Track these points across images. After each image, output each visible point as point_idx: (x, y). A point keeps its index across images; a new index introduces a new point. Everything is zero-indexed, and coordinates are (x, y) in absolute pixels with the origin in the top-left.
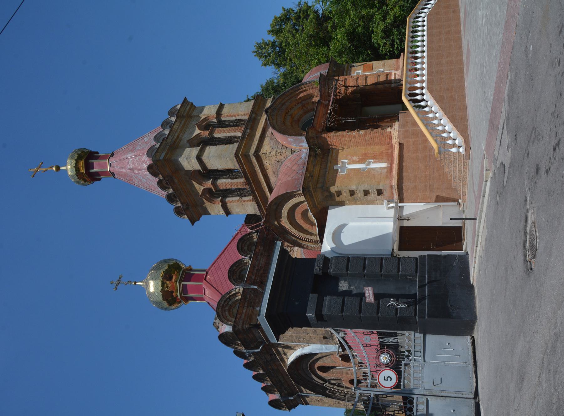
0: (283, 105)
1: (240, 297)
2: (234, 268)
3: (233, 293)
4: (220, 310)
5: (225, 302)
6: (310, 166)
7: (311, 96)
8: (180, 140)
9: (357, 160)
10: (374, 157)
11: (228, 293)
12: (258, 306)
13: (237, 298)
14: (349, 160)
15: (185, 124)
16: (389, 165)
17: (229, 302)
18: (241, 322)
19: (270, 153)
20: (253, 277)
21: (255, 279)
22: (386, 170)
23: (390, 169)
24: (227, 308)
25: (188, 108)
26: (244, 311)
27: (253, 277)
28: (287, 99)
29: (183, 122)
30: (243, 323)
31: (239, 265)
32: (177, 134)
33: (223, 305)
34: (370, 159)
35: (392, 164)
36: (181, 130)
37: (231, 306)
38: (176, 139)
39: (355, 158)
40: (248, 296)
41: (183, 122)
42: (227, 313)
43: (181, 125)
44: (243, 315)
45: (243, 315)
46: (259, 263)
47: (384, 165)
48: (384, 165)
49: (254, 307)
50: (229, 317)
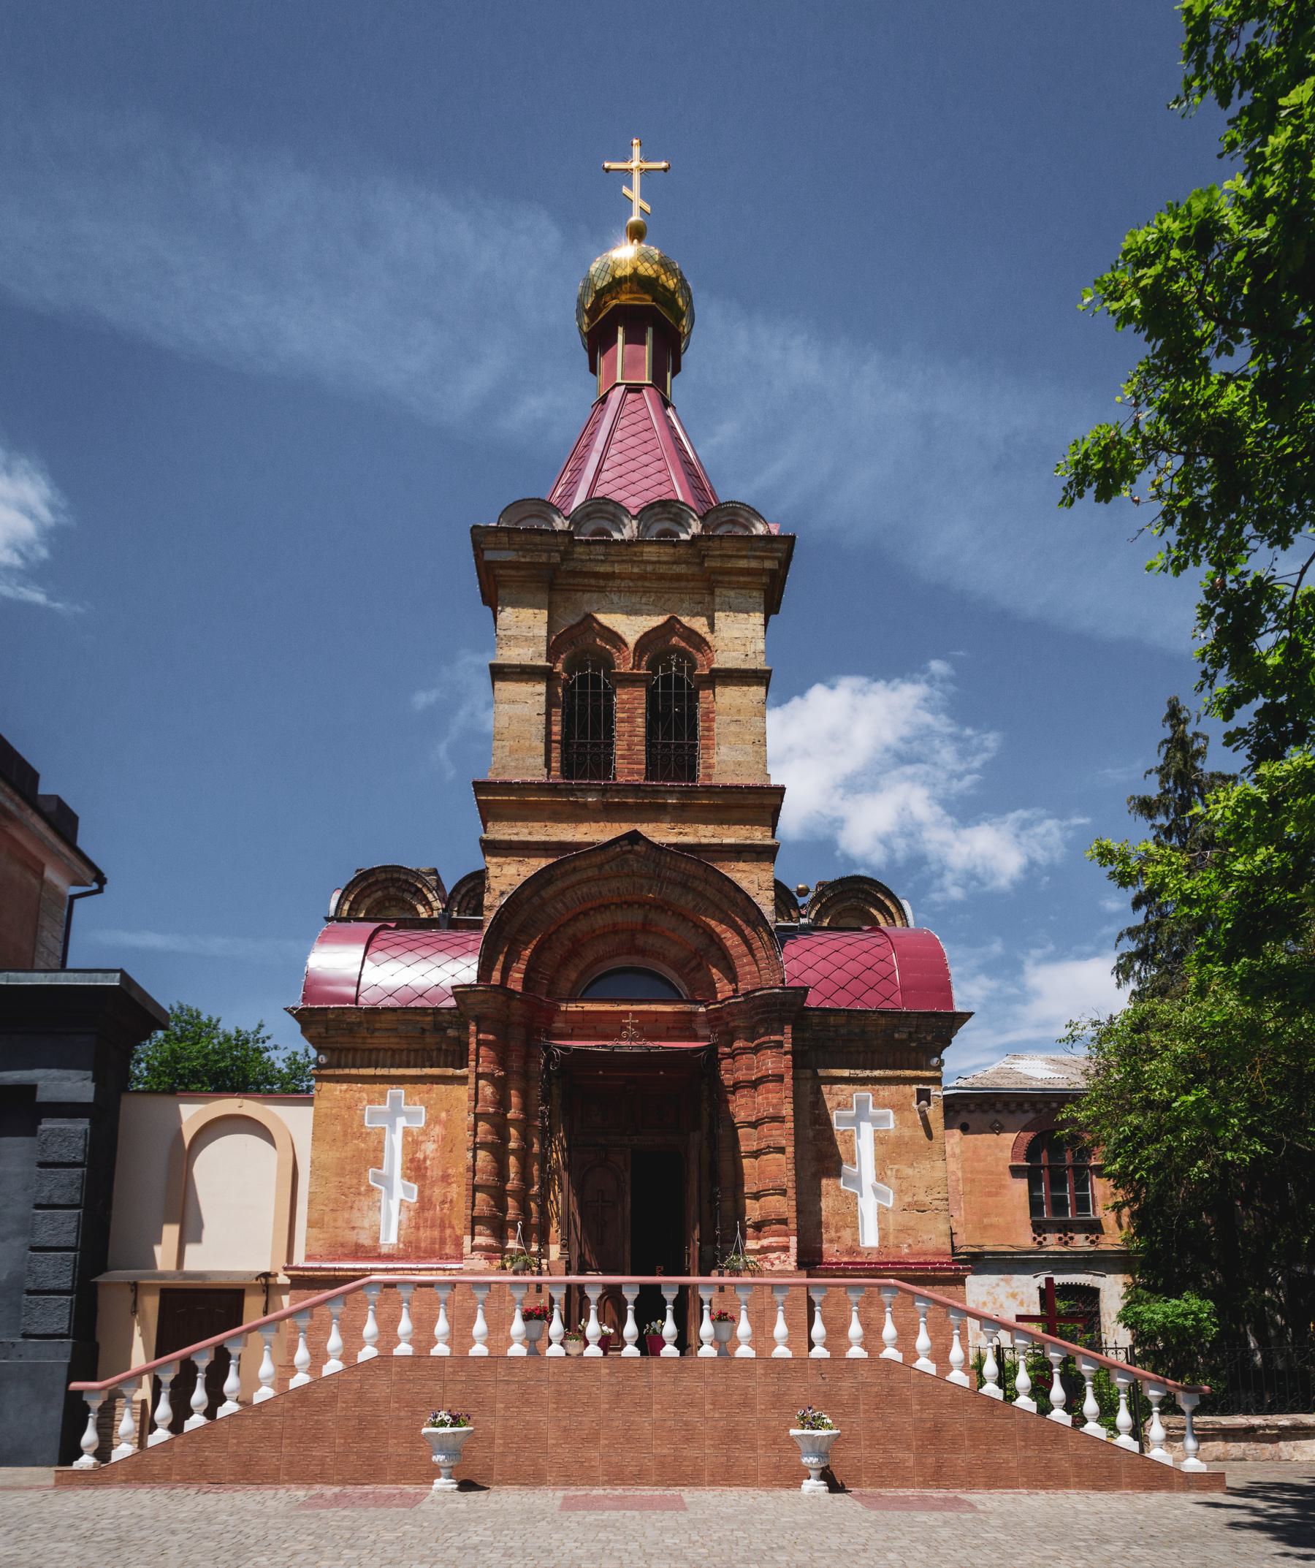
0: (684, 886)
6: (390, 1017)
7: (731, 975)
8: (601, 590)
9: (420, 1155)
10: (424, 1203)
14: (424, 1132)
15: (678, 578)
16: (384, 1250)
22: (365, 1240)
25: (742, 564)
29: (682, 569)
32: (617, 568)
34: (421, 1192)
35: (389, 1257)
36: (642, 577)
38: (597, 575)
39: (430, 1148)
41: (682, 569)
43: (662, 569)
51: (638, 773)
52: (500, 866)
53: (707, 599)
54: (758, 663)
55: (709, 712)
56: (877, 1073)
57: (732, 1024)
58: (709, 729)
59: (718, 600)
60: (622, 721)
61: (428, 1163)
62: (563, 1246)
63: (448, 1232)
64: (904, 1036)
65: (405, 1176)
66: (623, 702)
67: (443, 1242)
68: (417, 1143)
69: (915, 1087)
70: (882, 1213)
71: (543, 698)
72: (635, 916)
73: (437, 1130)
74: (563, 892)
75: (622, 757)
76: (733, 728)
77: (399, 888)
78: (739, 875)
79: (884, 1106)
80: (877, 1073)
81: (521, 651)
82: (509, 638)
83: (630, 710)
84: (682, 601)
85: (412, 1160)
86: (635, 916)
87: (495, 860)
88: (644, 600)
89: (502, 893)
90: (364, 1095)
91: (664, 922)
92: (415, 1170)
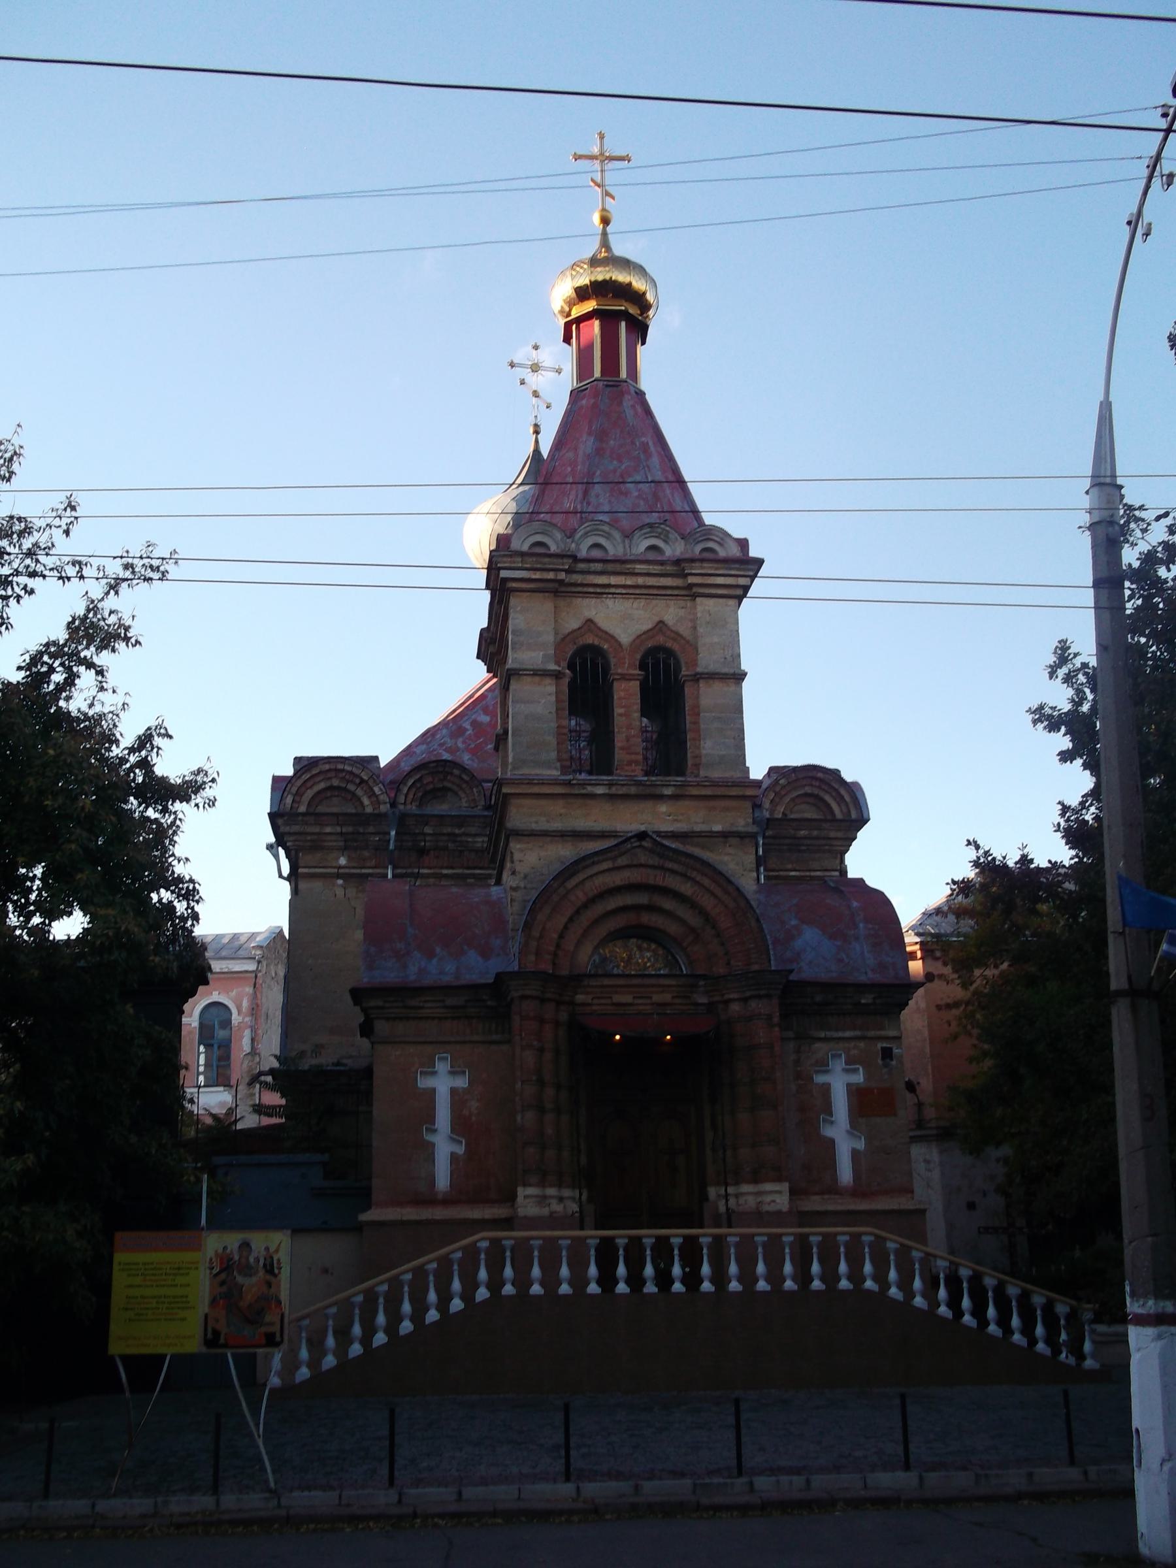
1: (369, 810)
2: (456, 772)
3: (376, 789)
4: (327, 767)
5: (351, 773)
8: (598, 595)
9: (466, 1112)
12: (350, 859)
13: (366, 801)
16: (440, 1197)
17: (352, 782)
18: (295, 828)
19: (514, 873)
20: (428, 830)
21: (425, 834)
23: (429, 1199)
24: (335, 783)
26: (328, 830)
27: (428, 830)
28: (706, 882)
30: (295, 834)
31: (466, 782)
33: (343, 770)
37: (345, 789)
39: (474, 1105)
40: (371, 829)
42: (322, 785)
44: (317, 829)
45: (317, 829)
46: (476, 835)
47: (443, 1181)
48: (443, 1181)
49: (345, 848)
50: (310, 794)
51: (637, 762)
52: (521, 850)
53: (689, 604)
55: (696, 706)
56: (848, 1034)
57: (726, 997)
58: (696, 723)
59: (699, 608)
60: (621, 715)
64: (870, 1001)
66: (620, 698)
69: (880, 1045)
70: (855, 1153)
71: (553, 698)
72: (642, 899)
74: (582, 882)
75: (622, 748)
77: (343, 778)
78: (726, 858)
79: (854, 1063)
80: (848, 1034)
81: (533, 654)
84: (668, 606)
86: (642, 899)
87: (518, 846)
88: (635, 605)
89: (525, 877)
91: (668, 904)
92: (461, 1126)
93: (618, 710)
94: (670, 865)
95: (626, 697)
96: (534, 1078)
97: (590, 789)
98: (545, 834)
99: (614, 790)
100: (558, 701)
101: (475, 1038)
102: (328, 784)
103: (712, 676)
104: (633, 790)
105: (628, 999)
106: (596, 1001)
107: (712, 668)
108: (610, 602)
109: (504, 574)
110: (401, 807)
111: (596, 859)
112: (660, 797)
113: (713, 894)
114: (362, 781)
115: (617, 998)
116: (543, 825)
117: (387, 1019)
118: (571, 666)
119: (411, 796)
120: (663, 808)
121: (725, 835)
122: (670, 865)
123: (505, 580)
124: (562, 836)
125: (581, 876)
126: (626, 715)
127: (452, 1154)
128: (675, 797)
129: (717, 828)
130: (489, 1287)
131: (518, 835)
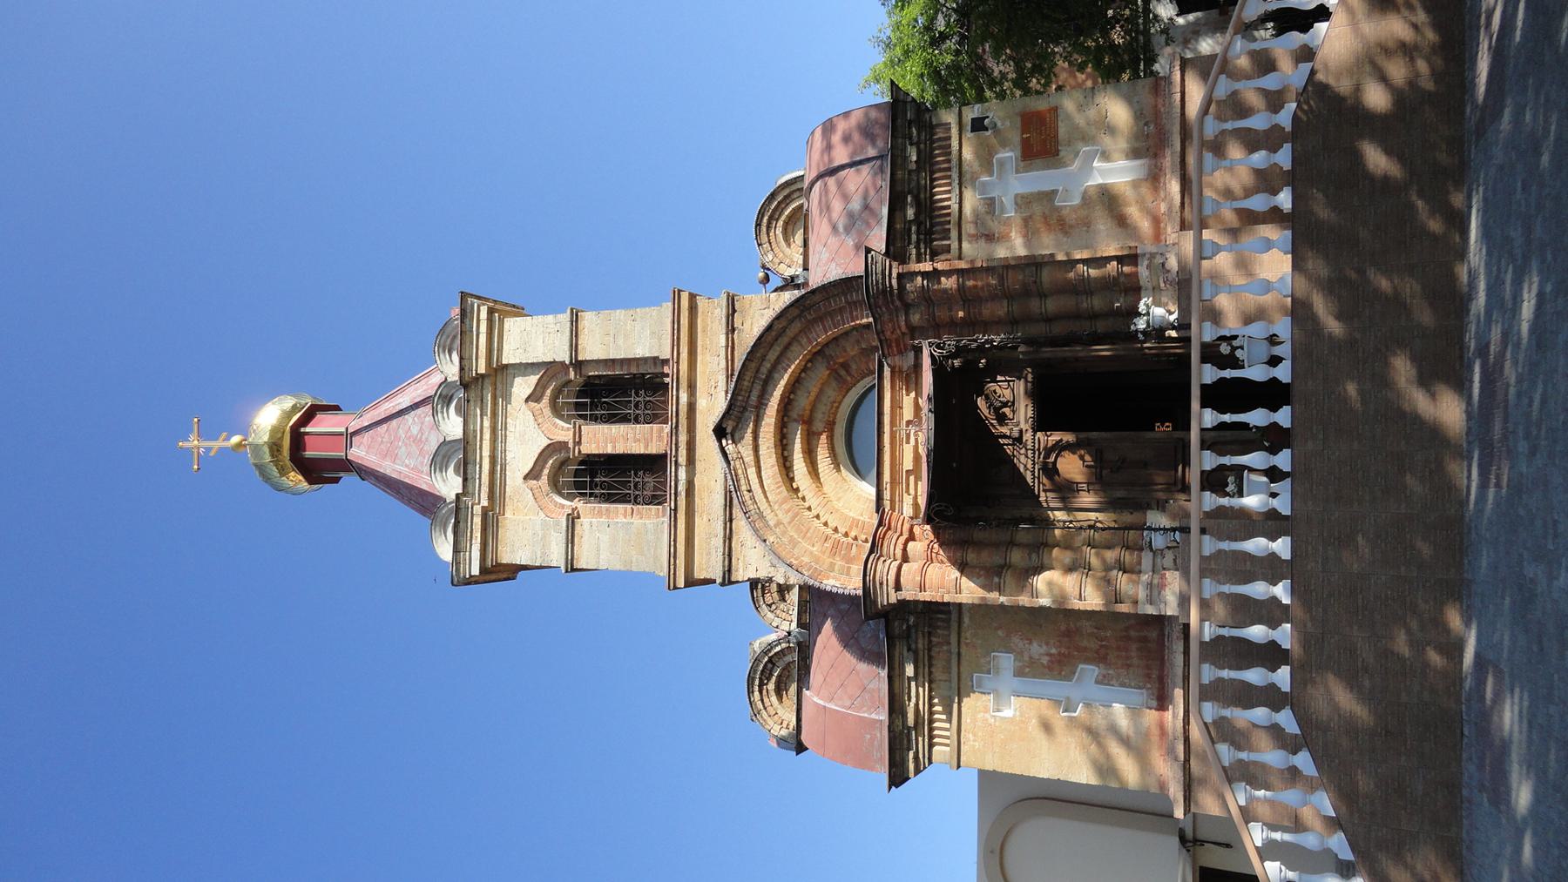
4: (757, 694)
8: (504, 470)
9: (1045, 660)
10: (1100, 658)
11: (765, 653)
14: (1019, 654)
39: (1037, 649)
51: (661, 430)
54: (565, 318)
57: (904, 329)
61: (1053, 651)
62: (1149, 507)
63: (1133, 633)
65: (1068, 678)
67: (1144, 640)
68: (1032, 662)
73: (1016, 640)
75: (646, 447)
76: (621, 342)
79: (990, 164)
82: (544, 554)
83: (605, 439)
85: (1050, 669)
90: (980, 715)
93: (609, 451)
94: (754, 398)
95: (605, 439)
96: (996, 580)
97: (682, 488)
98: (729, 538)
99: (682, 459)
100: (600, 514)
101: (954, 639)
102: (772, 693)
103: (574, 347)
104: (683, 438)
105: (908, 451)
106: (912, 491)
107: (567, 347)
108: (509, 456)
109: (476, 571)
110: (794, 625)
111: (744, 488)
112: (692, 407)
113: (787, 347)
114: (770, 660)
115: (908, 464)
116: (718, 542)
117: (931, 746)
118: (570, 497)
119: (784, 615)
120: (702, 403)
121: (731, 329)
122: (754, 398)
123: (483, 570)
124: (731, 521)
125: (763, 505)
126: (614, 441)
127: (1097, 682)
128: (692, 387)
129: (723, 341)
130: (1276, 708)
131: (729, 571)
